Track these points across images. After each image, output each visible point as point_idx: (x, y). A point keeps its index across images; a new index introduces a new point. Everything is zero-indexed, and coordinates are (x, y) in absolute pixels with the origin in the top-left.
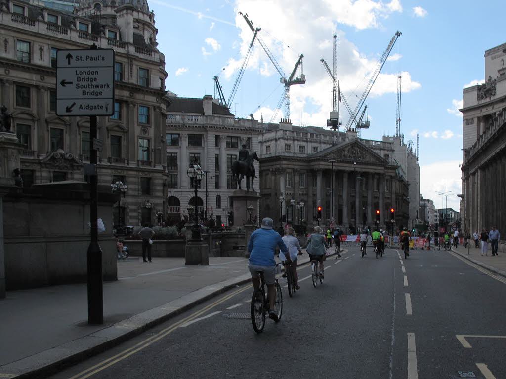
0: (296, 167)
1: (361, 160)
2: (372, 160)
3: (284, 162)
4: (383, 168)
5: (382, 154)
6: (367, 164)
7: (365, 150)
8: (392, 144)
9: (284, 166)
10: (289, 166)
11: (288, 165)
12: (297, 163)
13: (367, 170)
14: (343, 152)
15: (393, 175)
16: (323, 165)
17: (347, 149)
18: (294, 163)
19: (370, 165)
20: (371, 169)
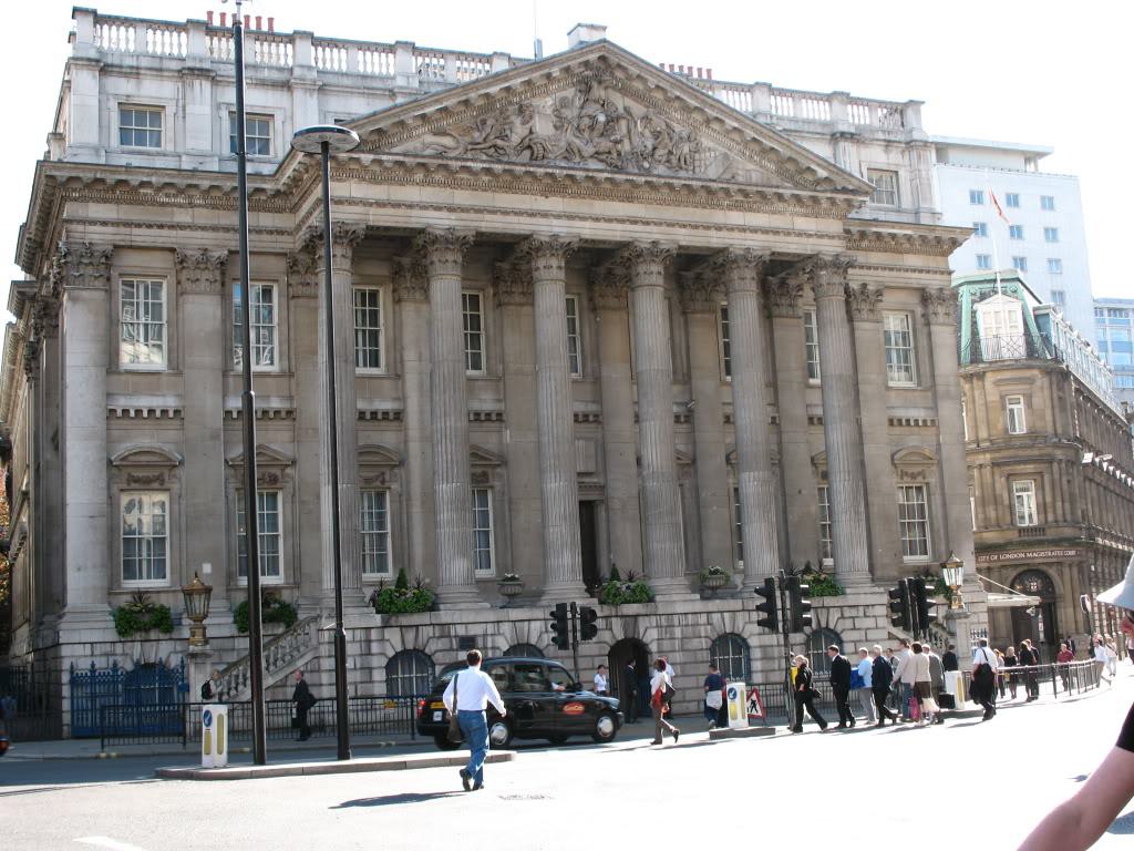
0: (193, 240)
1: (661, 169)
2: (750, 170)
3: (97, 210)
4: (835, 226)
5: (854, 161)
6: (710, 195)
7: (687, 109)
8: (910, 113)
9: (100, 236)
10: (142, 236)
11: (127, 224)
12: (204, 216)
13: (715, 240)
14: (517, 121)
15: (933, 282)
16: (359, 200)
17: (547, 103)
18: (183, 217)
19: (737, 207)
20: (743, 229)
